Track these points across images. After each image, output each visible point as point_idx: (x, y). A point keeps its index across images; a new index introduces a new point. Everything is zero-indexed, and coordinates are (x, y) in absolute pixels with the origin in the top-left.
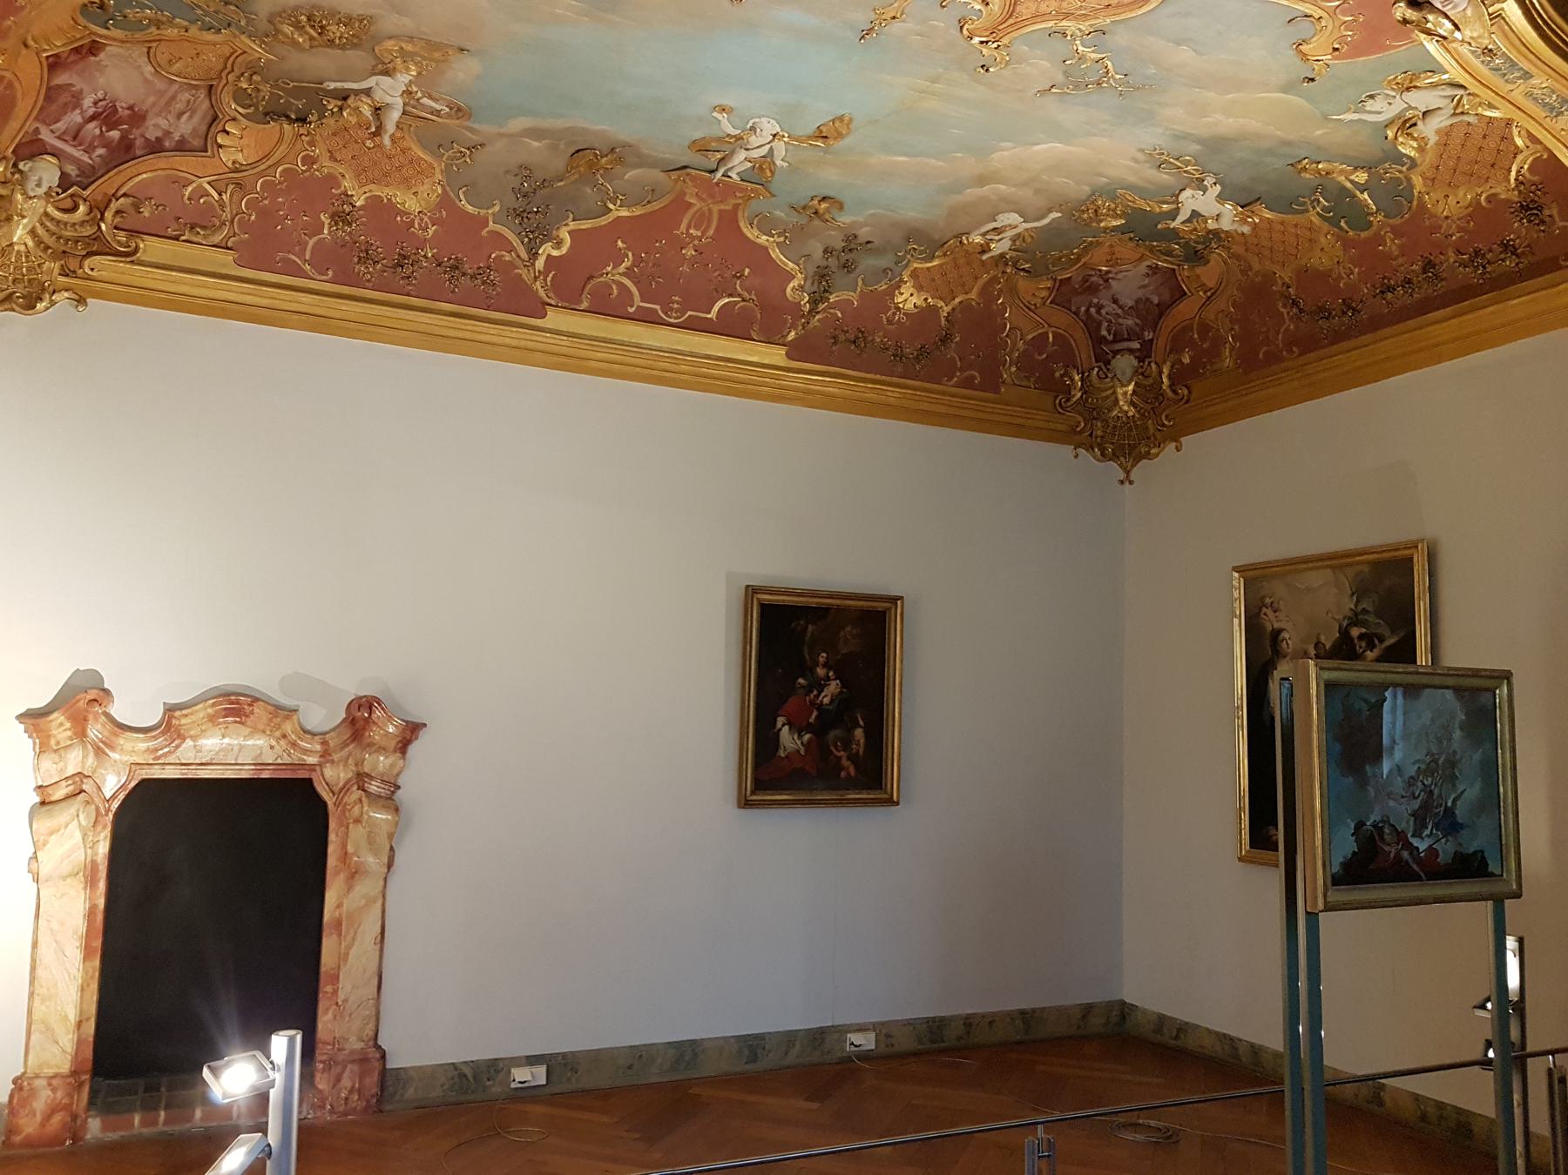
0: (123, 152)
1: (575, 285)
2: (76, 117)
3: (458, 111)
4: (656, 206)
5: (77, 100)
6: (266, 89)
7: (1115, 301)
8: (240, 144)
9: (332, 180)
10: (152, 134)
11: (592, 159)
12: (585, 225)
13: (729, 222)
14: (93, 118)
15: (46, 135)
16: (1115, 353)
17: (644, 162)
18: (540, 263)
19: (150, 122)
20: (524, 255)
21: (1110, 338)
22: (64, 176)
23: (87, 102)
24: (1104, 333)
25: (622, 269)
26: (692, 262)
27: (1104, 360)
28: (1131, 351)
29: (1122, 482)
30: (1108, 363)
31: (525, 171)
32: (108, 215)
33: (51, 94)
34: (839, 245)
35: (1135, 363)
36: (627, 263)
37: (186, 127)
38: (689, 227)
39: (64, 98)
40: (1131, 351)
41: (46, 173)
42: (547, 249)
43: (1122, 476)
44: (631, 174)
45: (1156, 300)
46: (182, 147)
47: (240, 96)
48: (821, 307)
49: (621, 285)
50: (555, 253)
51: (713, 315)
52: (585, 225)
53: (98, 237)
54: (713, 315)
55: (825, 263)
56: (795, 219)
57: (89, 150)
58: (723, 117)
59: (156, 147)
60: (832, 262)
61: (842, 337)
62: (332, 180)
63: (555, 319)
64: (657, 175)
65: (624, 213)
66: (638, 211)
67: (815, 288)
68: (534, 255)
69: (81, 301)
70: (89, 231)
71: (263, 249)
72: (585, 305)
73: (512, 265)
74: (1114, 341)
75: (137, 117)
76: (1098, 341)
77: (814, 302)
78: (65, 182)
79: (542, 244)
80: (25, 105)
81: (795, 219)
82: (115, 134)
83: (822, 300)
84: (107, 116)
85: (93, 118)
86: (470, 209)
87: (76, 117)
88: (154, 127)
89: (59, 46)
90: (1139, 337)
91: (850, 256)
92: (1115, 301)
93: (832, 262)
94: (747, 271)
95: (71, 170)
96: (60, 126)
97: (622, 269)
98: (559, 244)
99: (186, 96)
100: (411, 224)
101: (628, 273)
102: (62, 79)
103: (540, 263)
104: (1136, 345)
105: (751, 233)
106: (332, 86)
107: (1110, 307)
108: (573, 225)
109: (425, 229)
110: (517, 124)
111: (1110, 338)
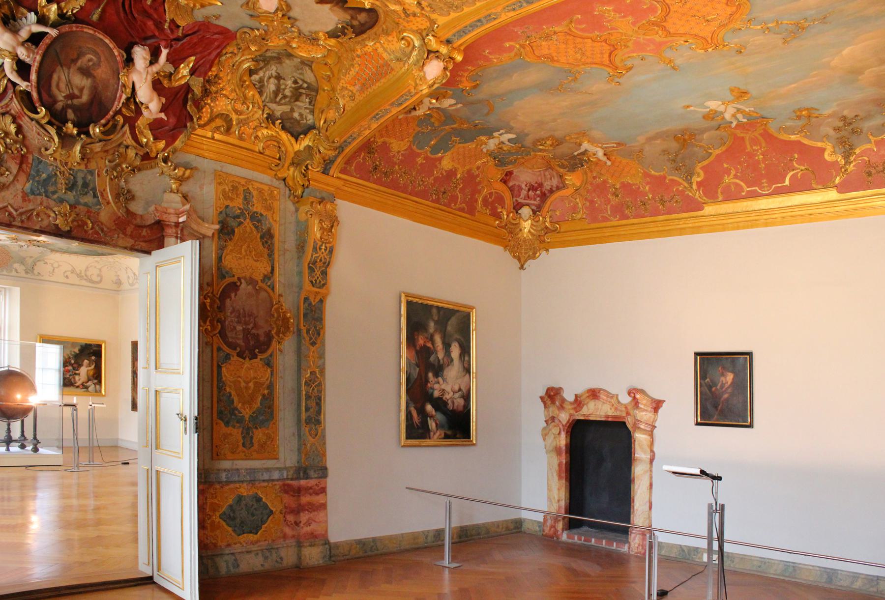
0: (544, 197)
1: (712, 188)
2: (524, 193)
3: (619, 144)
4: (728, 144)
5: (520, 188)
6: (563, 161)
8: (572, 179)
9: (605, 182)
10: (548, 188)
11: (685, 138)
12: (705, 163)
13: (768, 136)
14: (529, 190)
15: (520, 200)
17: (703, 131)
18: (695, 187)
19: (545, 184)
20: (686, 185)
22: (533, 210)
23: (524, 186)
25: (732, 176)
26: (764, 160)
31: (665, 152)
32: (548, 219)
33: (511, 189)
34: (841, 124)
36: (733, 172)
37: (555, 182)
38: (751, 147)
39: (516, 189)
41: (526, 211)
42: (696, 179)
44: (705, 136)
46: (558, 188)
47: (562, 166)
48: (852, 158)
49: (737, 185)
50: (699, 179)
51: (787, 182)
52: (705, 163)
53: (547, 228)
54: (787, 182)
55: (839, 136)
56: (800, 123)
57: (535, 200)
58: (692, 108)
59: (551, 191)
60: (843, 133)
61: (873, 171)
62: (605, 182)
63: (709, 209)
64: (714, 133)
65: (718, 152)
66: (724, 148)
67: (843, 150)
68: (691, 183)
69: (547, 250)
70: (543, 226)
71: (594, 214)
72: (720, 199)
73: (683, 191)
75: (541, 185)
77: (847, 156)
78: (534, 212)
79: (691, 177)
80: (507, 195)
81: (800, 123)
82: (538, 192)
83: (850, 155)
84: (532, 188)
85: (529, 190)
86: (657, 174)
87: (524, 193)
88: (547, 186)
89: (499, 177)
91: (851, 127)
93: (843, 133)
94: (796, 156)
95: (533, 207)
96: (522, 196)
97: (732, 176)
98: (699, 175)
99: (547, 173)
100: (639, 188)
101: (736, 177)
102: (511, 184)
103: (695, 187)
105: (784, 137)
106: (576, 153)
108: (700, 165)
109: (644, 188)
110: (641, 139)
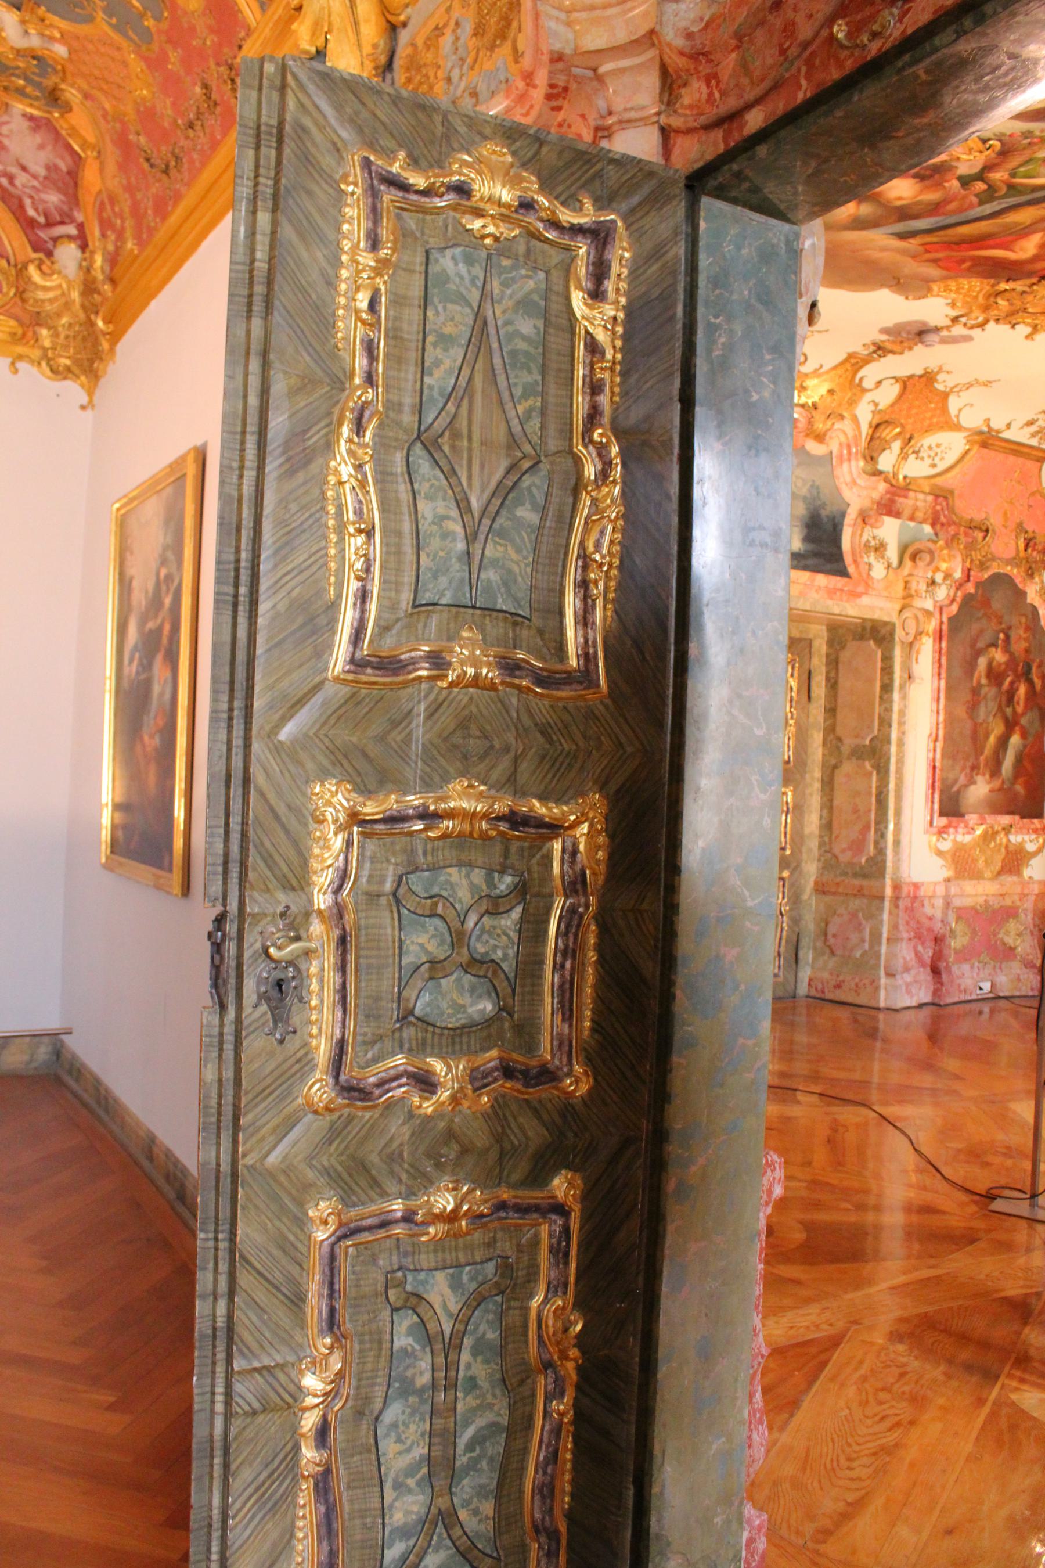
7: (24, 169)
16: (55, 240)
21: (42, 220)
24: (31, 213)
27: (45, 250)
28: (70, 238)
29: (83, 407)
30: (49, 254)
35: (78, 254)
40: (70, 238)
43: (84, 399)
45: (64, 168)
74: (49, 224)
76: (29, 225)
90: (73, 220)
92: (24, 169)
104: (72, 230)
107: (21, 179)
111: (42, 220)
